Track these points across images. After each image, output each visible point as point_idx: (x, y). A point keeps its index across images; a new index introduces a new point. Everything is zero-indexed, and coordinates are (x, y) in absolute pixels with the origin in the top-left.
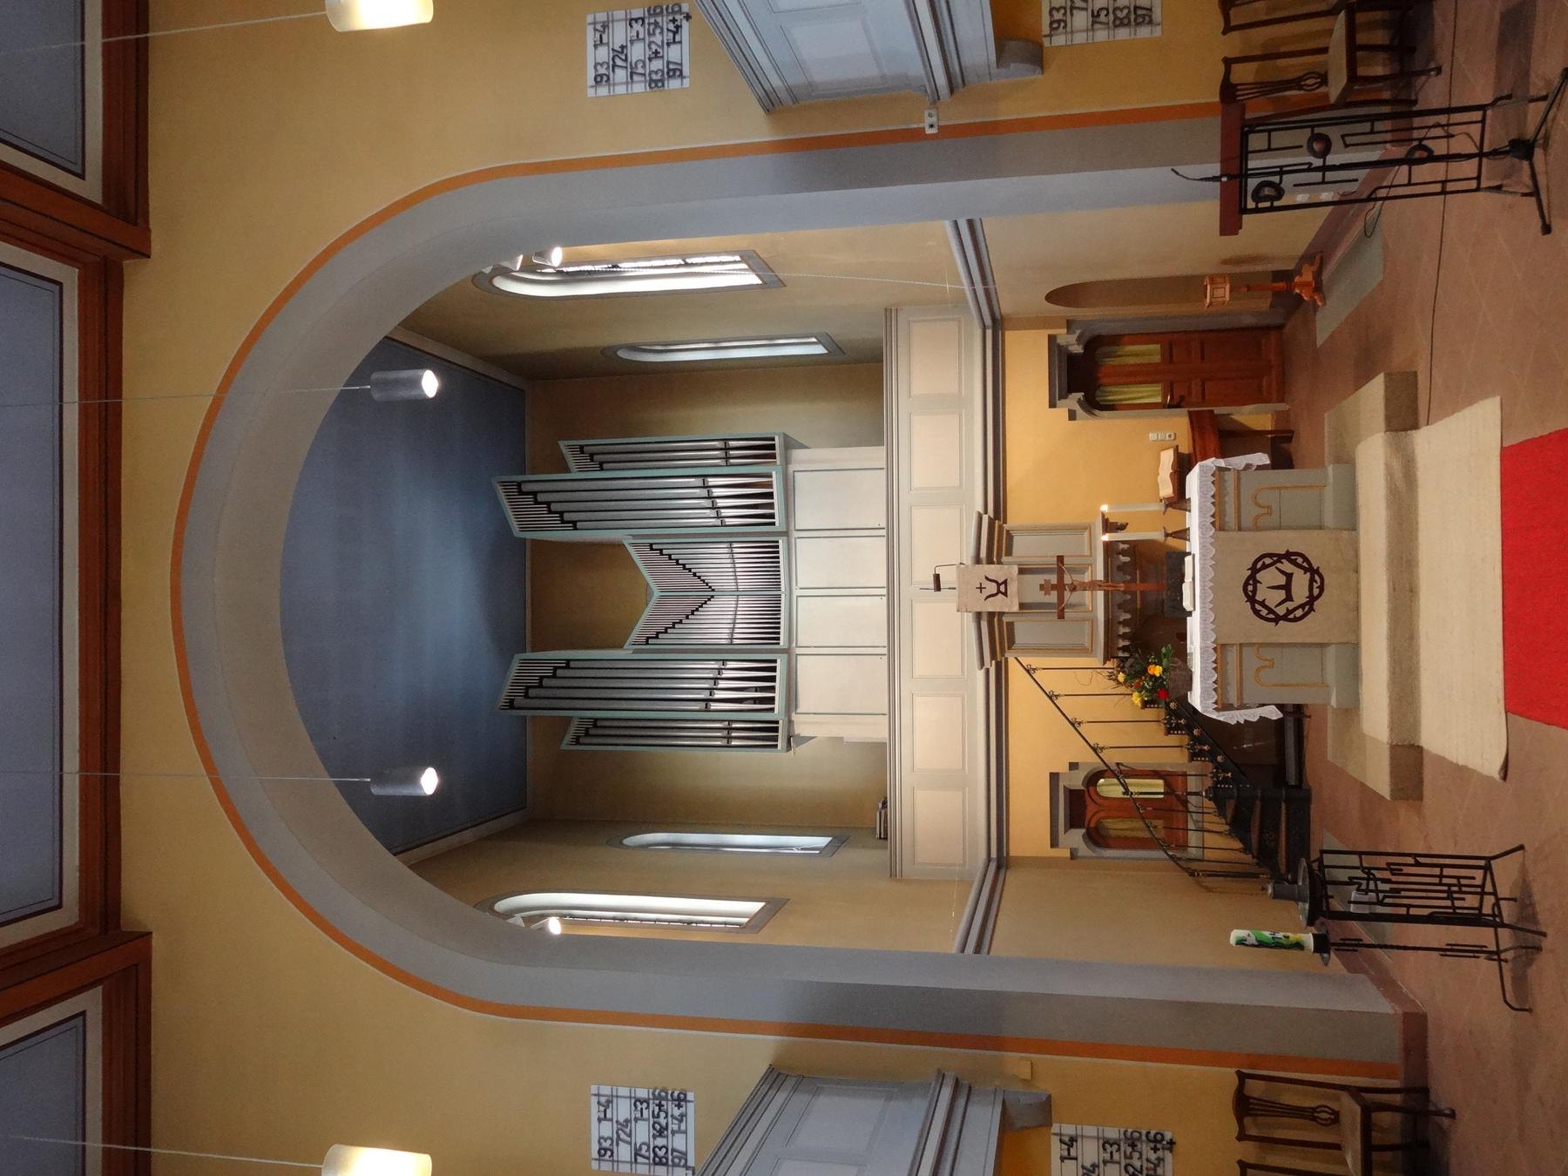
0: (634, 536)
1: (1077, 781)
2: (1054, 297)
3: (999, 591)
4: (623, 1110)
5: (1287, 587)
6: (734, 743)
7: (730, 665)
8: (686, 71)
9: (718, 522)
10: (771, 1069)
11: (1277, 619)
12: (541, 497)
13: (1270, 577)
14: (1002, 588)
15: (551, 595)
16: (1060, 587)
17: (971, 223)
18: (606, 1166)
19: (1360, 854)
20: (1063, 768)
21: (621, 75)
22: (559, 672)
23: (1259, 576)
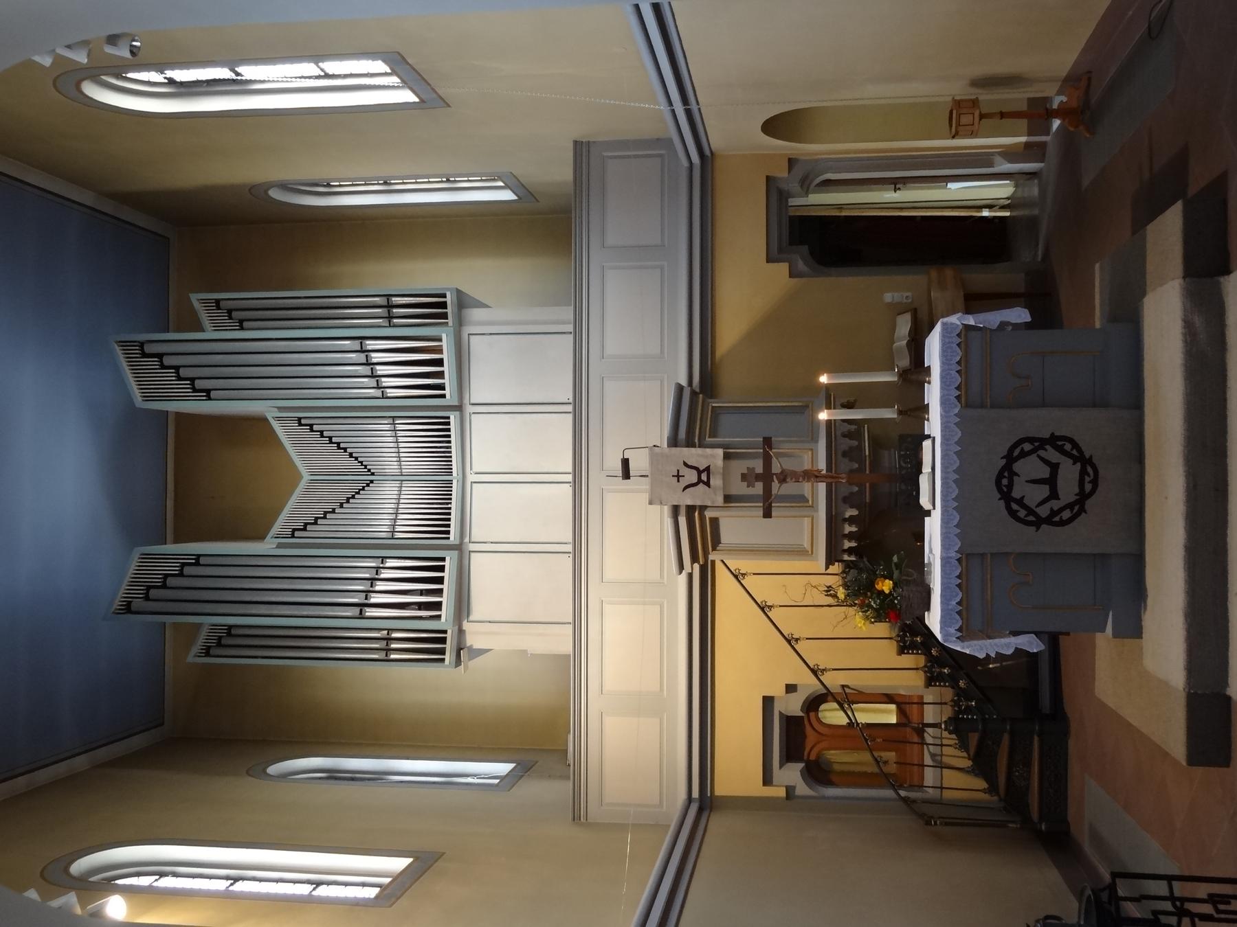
0: (281, 409)
1: (794, 705)
2: (772, 127)
3: (700, 481)
5: (1051, 481)
9: (378, 393)
11: (1038, 522)
12: (167, 361)
13: (1030, 468)
14: (703, 476)
15: (191, 477)
16: (766, 477)
17: (656, 8)
19: (1169, 879)
20: (778, 691)
22: (187, 570)
23: (1017, 467)
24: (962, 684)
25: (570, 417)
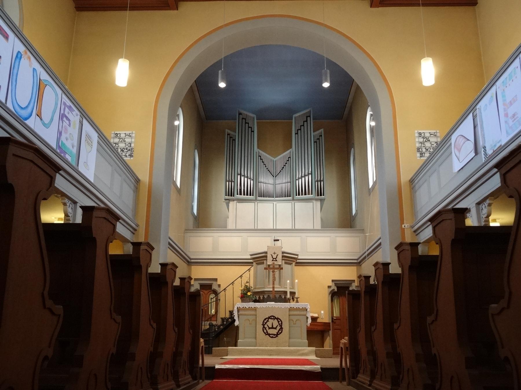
1: (215, 287)
4: (128, 140)
5: (272, 328)
6: (227, 183)
7: (252, 182)
8: (422, 158)
9: (297, 178)
10: (139, 180)
11: (263, 325)
12: (305, 123)
16: (274, 268)
20: (219, 283)
21: (421, 140)
22: (250, 129)
23: (276, 320)
24: (222, 327)
25: (291, 228)
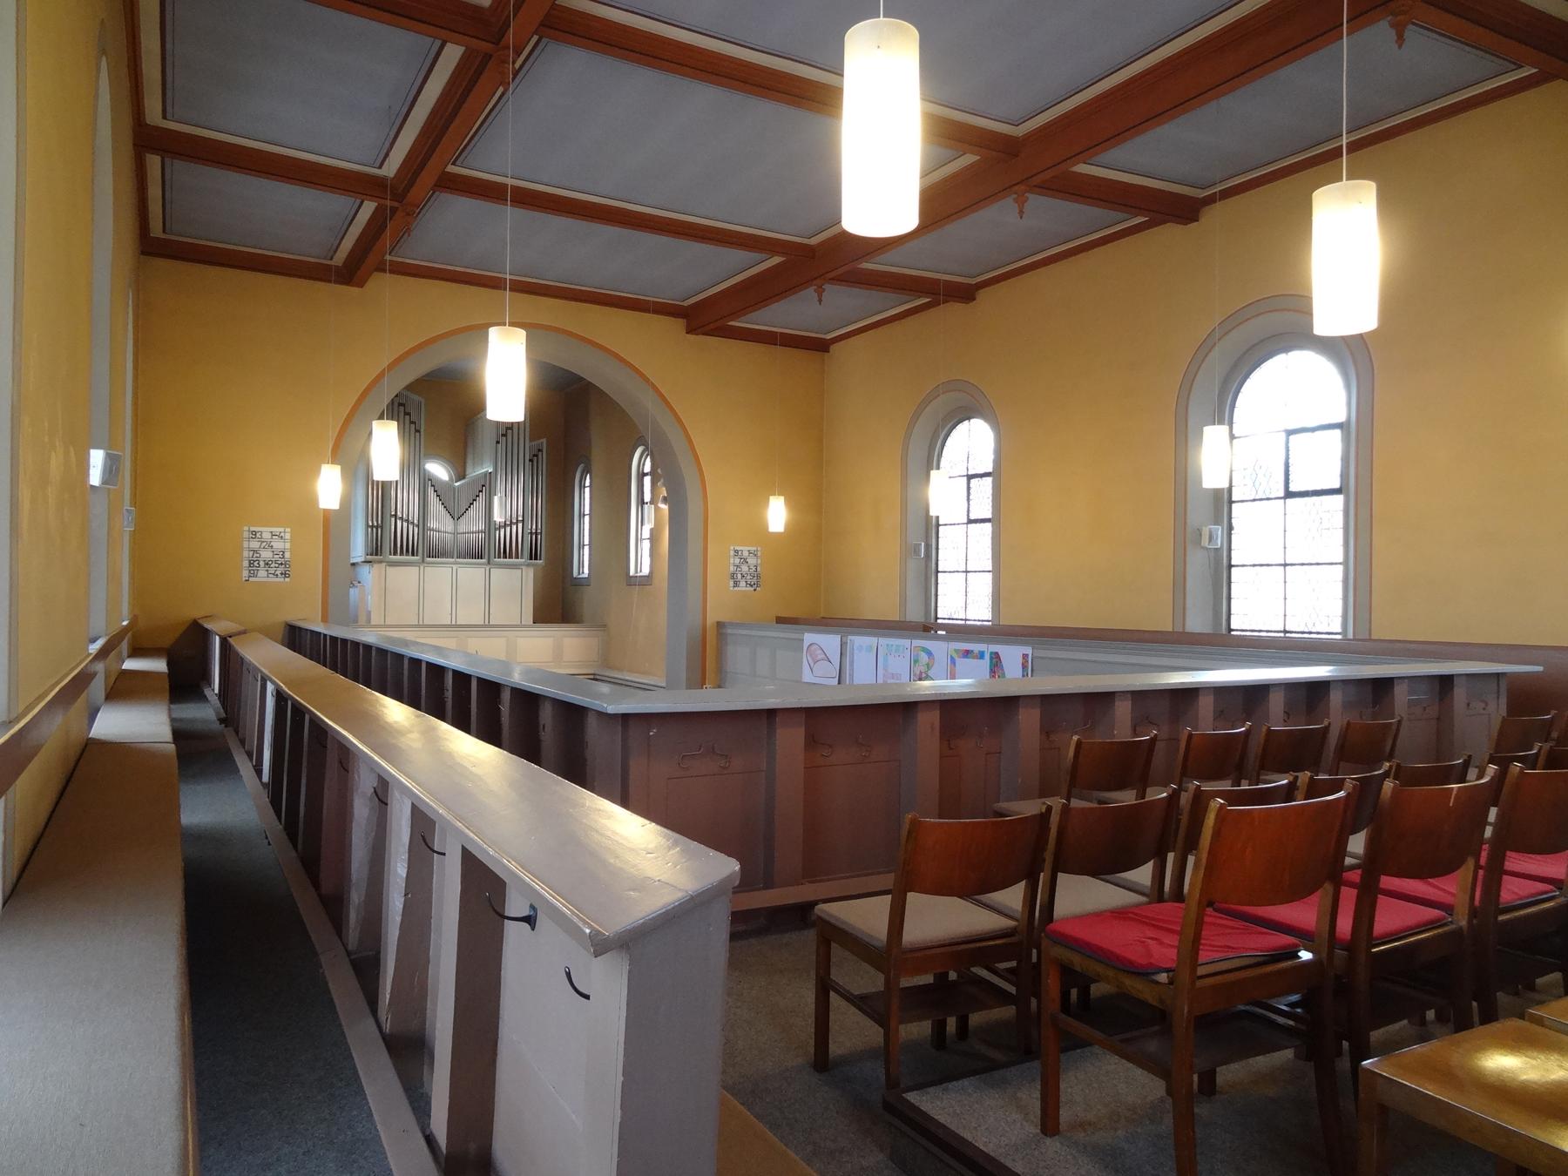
4: (278, 545)
18: (246, 534)
